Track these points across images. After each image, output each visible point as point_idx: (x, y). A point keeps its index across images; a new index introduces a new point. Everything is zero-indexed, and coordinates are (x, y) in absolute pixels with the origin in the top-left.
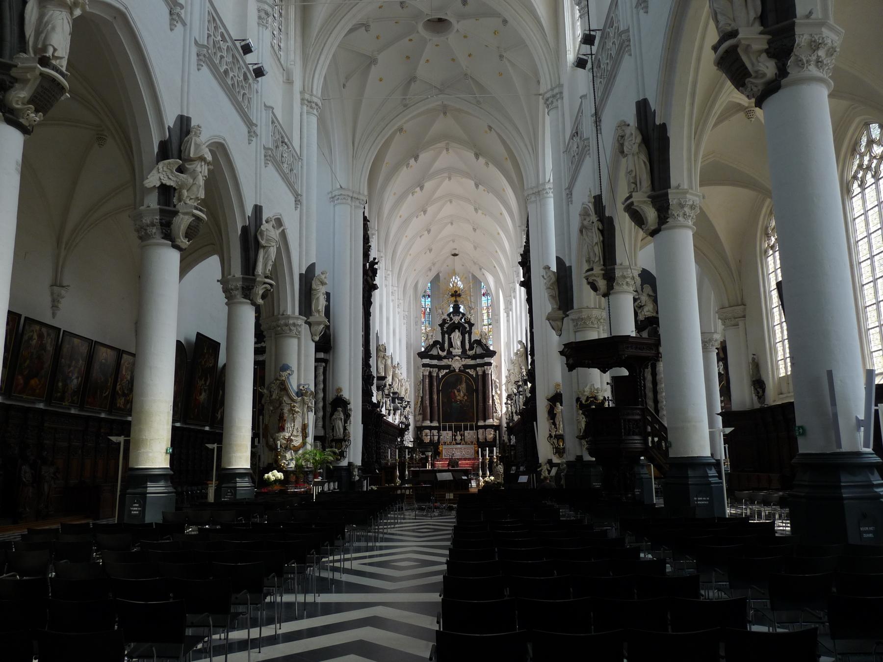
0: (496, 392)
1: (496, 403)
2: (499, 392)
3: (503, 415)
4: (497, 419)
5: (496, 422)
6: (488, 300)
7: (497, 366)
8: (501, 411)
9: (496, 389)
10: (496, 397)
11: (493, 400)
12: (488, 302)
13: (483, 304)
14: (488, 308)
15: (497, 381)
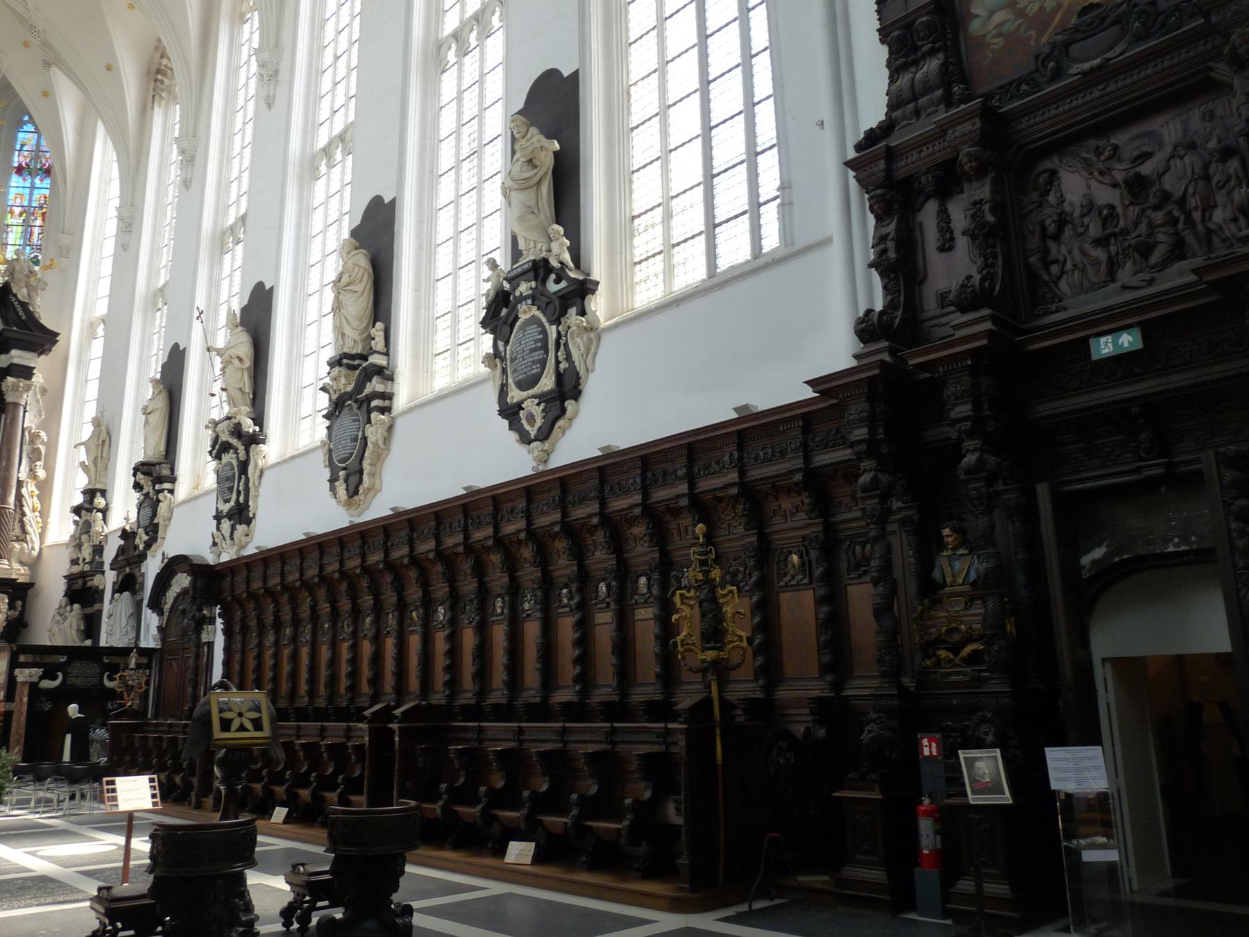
0: (32, 473)
1: (26, 509)
2: (41, 474)
3: (45, 552)
4: (21, 563)
5: (19, 573)
6: (33, 187)
7: (44, 391)
8: (42, 536)
9: (32, 461)
10: (30, 489)
11: (19, 497)
12: (31, 194)
13: (11, 196)
14: (28, 212)
15: (43, 434)
